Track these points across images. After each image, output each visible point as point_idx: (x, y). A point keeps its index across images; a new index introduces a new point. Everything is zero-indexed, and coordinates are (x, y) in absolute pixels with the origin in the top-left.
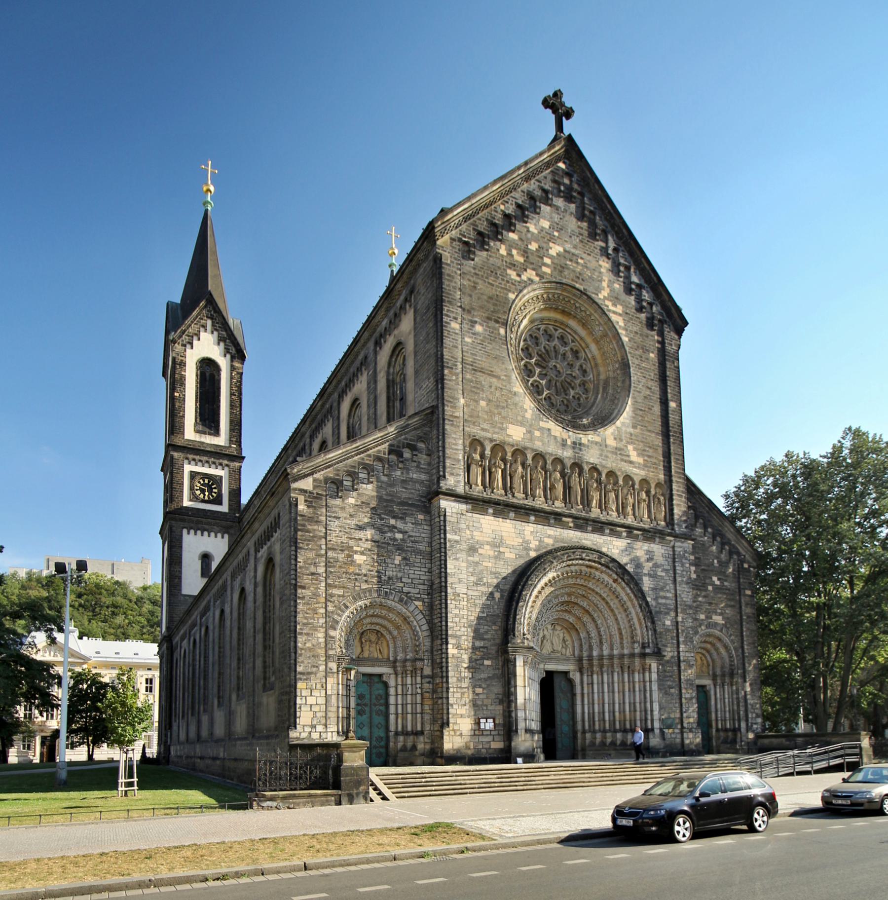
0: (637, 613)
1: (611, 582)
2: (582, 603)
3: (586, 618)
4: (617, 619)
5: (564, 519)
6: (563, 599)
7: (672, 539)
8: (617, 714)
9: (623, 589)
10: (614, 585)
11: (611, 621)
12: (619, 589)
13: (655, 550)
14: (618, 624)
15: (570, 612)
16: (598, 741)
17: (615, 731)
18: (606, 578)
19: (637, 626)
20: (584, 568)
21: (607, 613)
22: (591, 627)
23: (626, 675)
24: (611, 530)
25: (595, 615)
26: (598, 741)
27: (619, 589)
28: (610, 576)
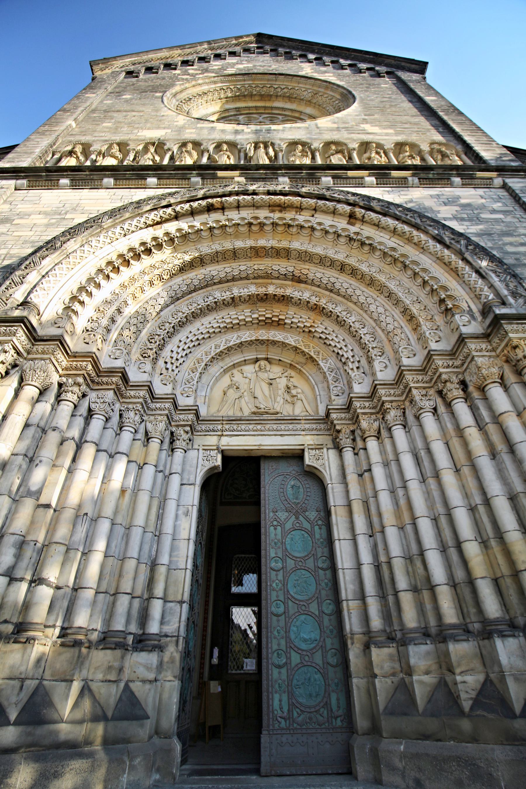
0: (440, 260)
1: (342, 224)
2: (296, 295)
3: (322, 326)
4: (390, 295)
5: (220, 173)
6: (245, 292)
7: (493, 174)
8: (472, 549)
9: (377, 225)
10: (353, 229)
11: (378, 304)
12: (368, 231)
13: (457, 194)
14: (397, 302)
15: (279, 324)
16: (422, 683)
17: (488, 631)
18: (327, 221)
19: (445, 278)
20: (263, 214)
21: (362, 292)
22: (338, 338)
23: (461, 408)
24: (334, 177)
25: (338, 310)
26: (422, 683)
27: (368, 231)
28: (334, 212)
